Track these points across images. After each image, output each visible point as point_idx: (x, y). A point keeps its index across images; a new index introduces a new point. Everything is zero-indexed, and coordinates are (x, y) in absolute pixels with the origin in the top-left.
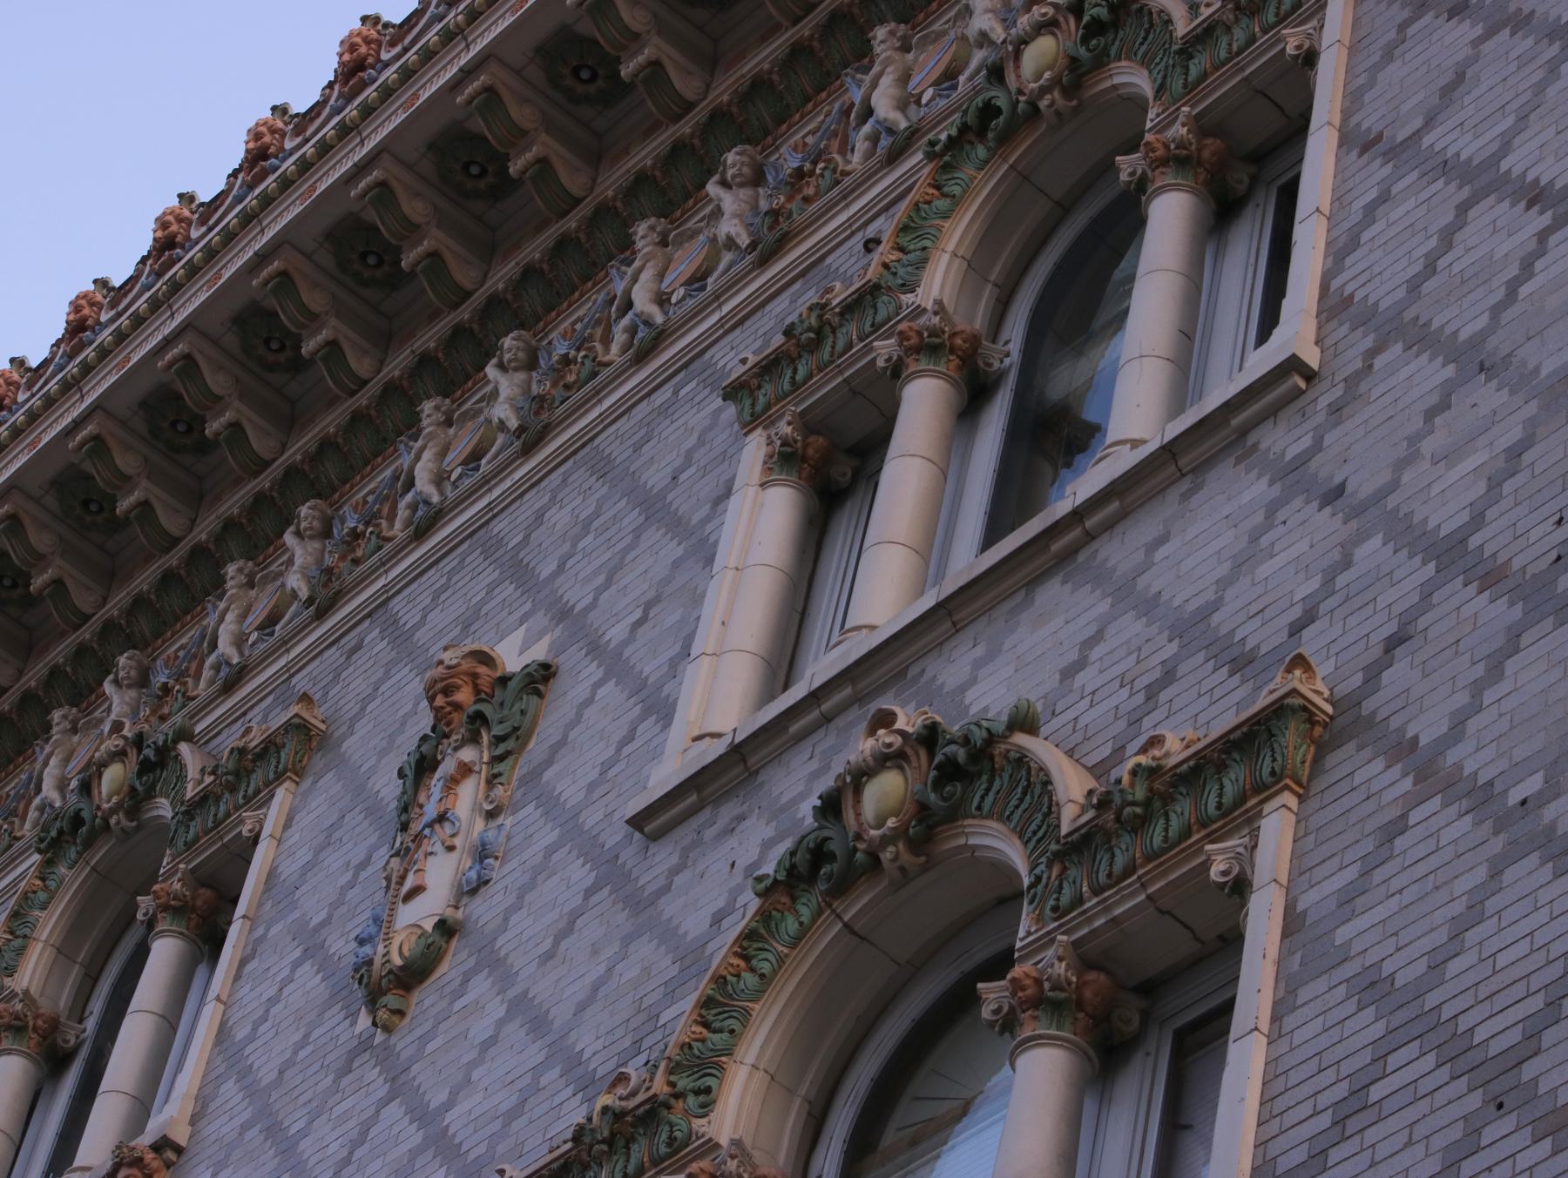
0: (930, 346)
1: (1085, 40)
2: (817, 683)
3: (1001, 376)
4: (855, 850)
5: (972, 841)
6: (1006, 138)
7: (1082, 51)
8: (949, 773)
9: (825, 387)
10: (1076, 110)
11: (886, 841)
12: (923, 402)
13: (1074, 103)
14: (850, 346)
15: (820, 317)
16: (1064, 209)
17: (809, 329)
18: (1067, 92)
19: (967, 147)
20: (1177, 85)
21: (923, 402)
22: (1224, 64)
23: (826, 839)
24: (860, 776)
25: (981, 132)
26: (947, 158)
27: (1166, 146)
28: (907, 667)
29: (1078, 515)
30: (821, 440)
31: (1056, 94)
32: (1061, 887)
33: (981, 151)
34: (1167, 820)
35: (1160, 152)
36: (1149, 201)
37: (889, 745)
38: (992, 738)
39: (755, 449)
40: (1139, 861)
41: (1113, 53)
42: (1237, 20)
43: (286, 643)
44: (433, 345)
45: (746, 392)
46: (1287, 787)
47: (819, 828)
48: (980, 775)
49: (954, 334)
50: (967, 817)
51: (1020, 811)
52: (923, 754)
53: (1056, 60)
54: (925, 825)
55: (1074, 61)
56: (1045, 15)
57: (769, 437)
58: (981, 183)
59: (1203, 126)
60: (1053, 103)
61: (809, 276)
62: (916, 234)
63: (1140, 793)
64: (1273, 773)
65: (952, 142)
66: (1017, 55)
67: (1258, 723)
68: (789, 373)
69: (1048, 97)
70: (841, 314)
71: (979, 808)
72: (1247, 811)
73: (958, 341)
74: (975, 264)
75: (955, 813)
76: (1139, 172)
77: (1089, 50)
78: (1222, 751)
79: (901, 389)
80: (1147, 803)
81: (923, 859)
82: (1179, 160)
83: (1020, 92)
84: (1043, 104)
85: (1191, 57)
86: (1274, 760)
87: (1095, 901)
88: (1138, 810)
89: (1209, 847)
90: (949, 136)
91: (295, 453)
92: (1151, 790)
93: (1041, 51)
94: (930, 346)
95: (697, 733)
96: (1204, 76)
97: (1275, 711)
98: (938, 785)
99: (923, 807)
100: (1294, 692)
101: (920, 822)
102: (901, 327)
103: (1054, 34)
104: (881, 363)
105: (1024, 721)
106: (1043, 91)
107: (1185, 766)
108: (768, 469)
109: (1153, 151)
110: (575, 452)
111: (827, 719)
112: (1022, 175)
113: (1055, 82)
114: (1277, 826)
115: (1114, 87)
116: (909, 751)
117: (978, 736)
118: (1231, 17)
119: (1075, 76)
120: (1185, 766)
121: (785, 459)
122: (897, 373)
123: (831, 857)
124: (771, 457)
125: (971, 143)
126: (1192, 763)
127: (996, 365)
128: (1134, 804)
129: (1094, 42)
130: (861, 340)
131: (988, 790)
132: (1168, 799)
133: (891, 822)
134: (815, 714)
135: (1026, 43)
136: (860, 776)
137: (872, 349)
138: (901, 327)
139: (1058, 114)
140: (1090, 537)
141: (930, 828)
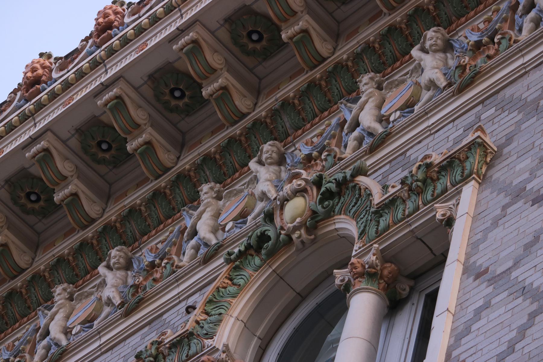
1: (321, 202)
7: (319, 207)
10: (313, 241)
13: (312, 237)
20: (372, 231)
22: (400, 222)
31: (303, 231)
42: (409, 197)
53: (304, 211)
55: (314, 213)
56: (300, 185)
59: (385, 256)
69: (298, 232)
82: (370, 274)
84: (295, 236)
93: (296, 207)
103: (304, 197)
109: (356, 268)
115: (336, 230)
118: (406, 195)
119: (314, 221)
129: (326, 203)
135: (288, 200)
139: (303, 242)
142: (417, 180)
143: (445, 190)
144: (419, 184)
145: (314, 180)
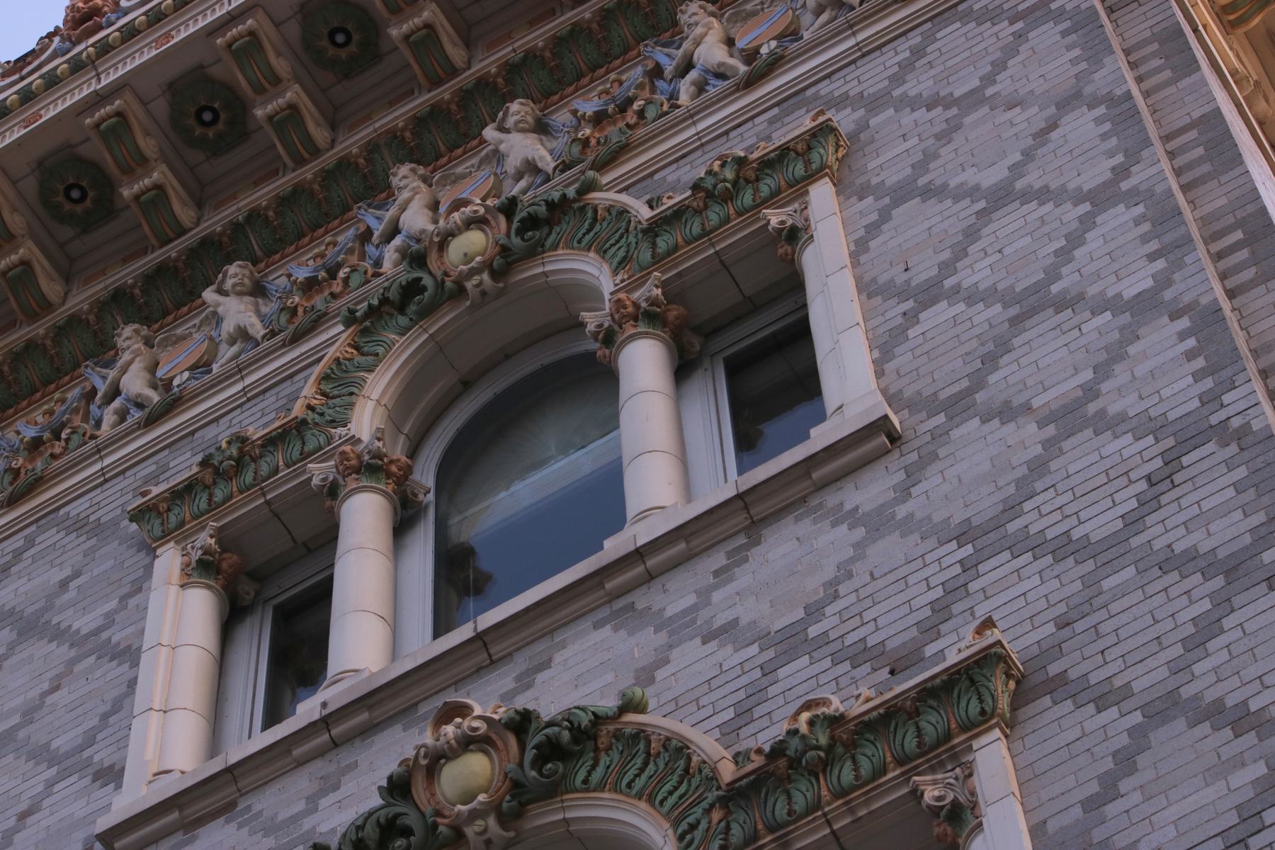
0: (371, 468)
1: (520, 232)
2: (641, 541)
3: (427, 507)
4: (435, 826)
5: (569, 815)
6: (427, 312)
7: (516, 241)
8: (551, 751)
9: (245, 507)
10: (500, 294)
11: (474, 815)
12: (364, 514)
13: (501, 285)
14: (276, 471)
15: (240, 450)
16: (467, 384)
17: (230, 458)
18: (496, 275)
19: (387, 317)
20: (646, 255)
21: (364, 514)
22: (697, 240)
23: (397, 816)
24: (436, 760)
25: (402, 309)
26: (367, 323)
27: (359, 457)
28: (416, 704)
29: (639, 554)
30: (235, 557)
31: (486, 276)
32: (728, 828)
33: (403, 321)
34: (789, 797)
35: (630, 309)
36: (802, 250)
37: (476, 729)
38: (599, 719)
39: (170, 560)
40: (824, 800)
41: (548, 243)
42: (706, 207)
43: (692, 116)
44: (493, 70)
45: (154, 514)
46: (997, 725)
47: (388, 805)
48: (581, 754)
49: (391, 462)
50: (567, 792)
51: (644, 777)
52: (512, 741)
53: (486, 248)
54: (517, 799)
55: (505, 250)
56: (476, 212)
57: (183, 549)
58: (401, 351)
59: (673, 292)
60: (480, 284)
61: (173, 448)
62: (341, 383)
63: (823, 740)
64: (983, 712)
65: (372, 311)
66: (442, 246)
67: (958, 672)
68: (205, 496)
69: (477, 277)
70: (263, 446)
71: (585, 781)
72: (953, 747)
73: (394, 468)
74: (398, 411)
75: (553, 790)
76: (331, 478)
77: (523, 240)
78: (914, 700)
79: (340, 507)
80: (830, 749)
81: (512, 834)
82: (651, 317)
83: (446, 274)
84: (469, 285)
85: (657, 236)
86: (981, 701)
87: (898, 772)
88: (822, 754)
89: (916, 778)
90: (370, 306)
91: (396, 118)
92: (832, 738)
93: (474, 241)
94: (371, 468)
95: (155, 770)
96: (676, 248)
97: (976, 662)
98: (539, 763)
99: (517, 786)
100: (999, 643)
101: (513, 797)
102: (341, 449)
104: (316, 481)
105: (630, 705)
106: (473, 272)
107: (875, 713)
108: (186, 571)
109: (625, 307)
110: (739, 125)
111: (335, 744)
112: (439, 347)
113: (488, 265)
114: (992, 759)
115: (545, 274)
116: (494, 737)
117: (585, 720)
118: (701, 204)
119: (503, 263)
120: (875, 713)
121: (204, 568)
122: (333, 491)
123: (407, 832)
124: (188, 565)
125: (391, 315)
126: (752, 777)
127: (421, 497)
128: (818, 748)
129: (530, 233)
130: (288, 466)
131: (594, 767)
132: (851, 746)
133: (482, 797)
134: (639, 569)
135: (454, 236)
136: (436, 760)
137: (304, 472)
138: (341, 449)
139: (484, 293)
140: (650, 577)
141: (523, 805)
142: (725, 180)
143: (776, 193)
144: (728, 185)
145: (503, 204)
